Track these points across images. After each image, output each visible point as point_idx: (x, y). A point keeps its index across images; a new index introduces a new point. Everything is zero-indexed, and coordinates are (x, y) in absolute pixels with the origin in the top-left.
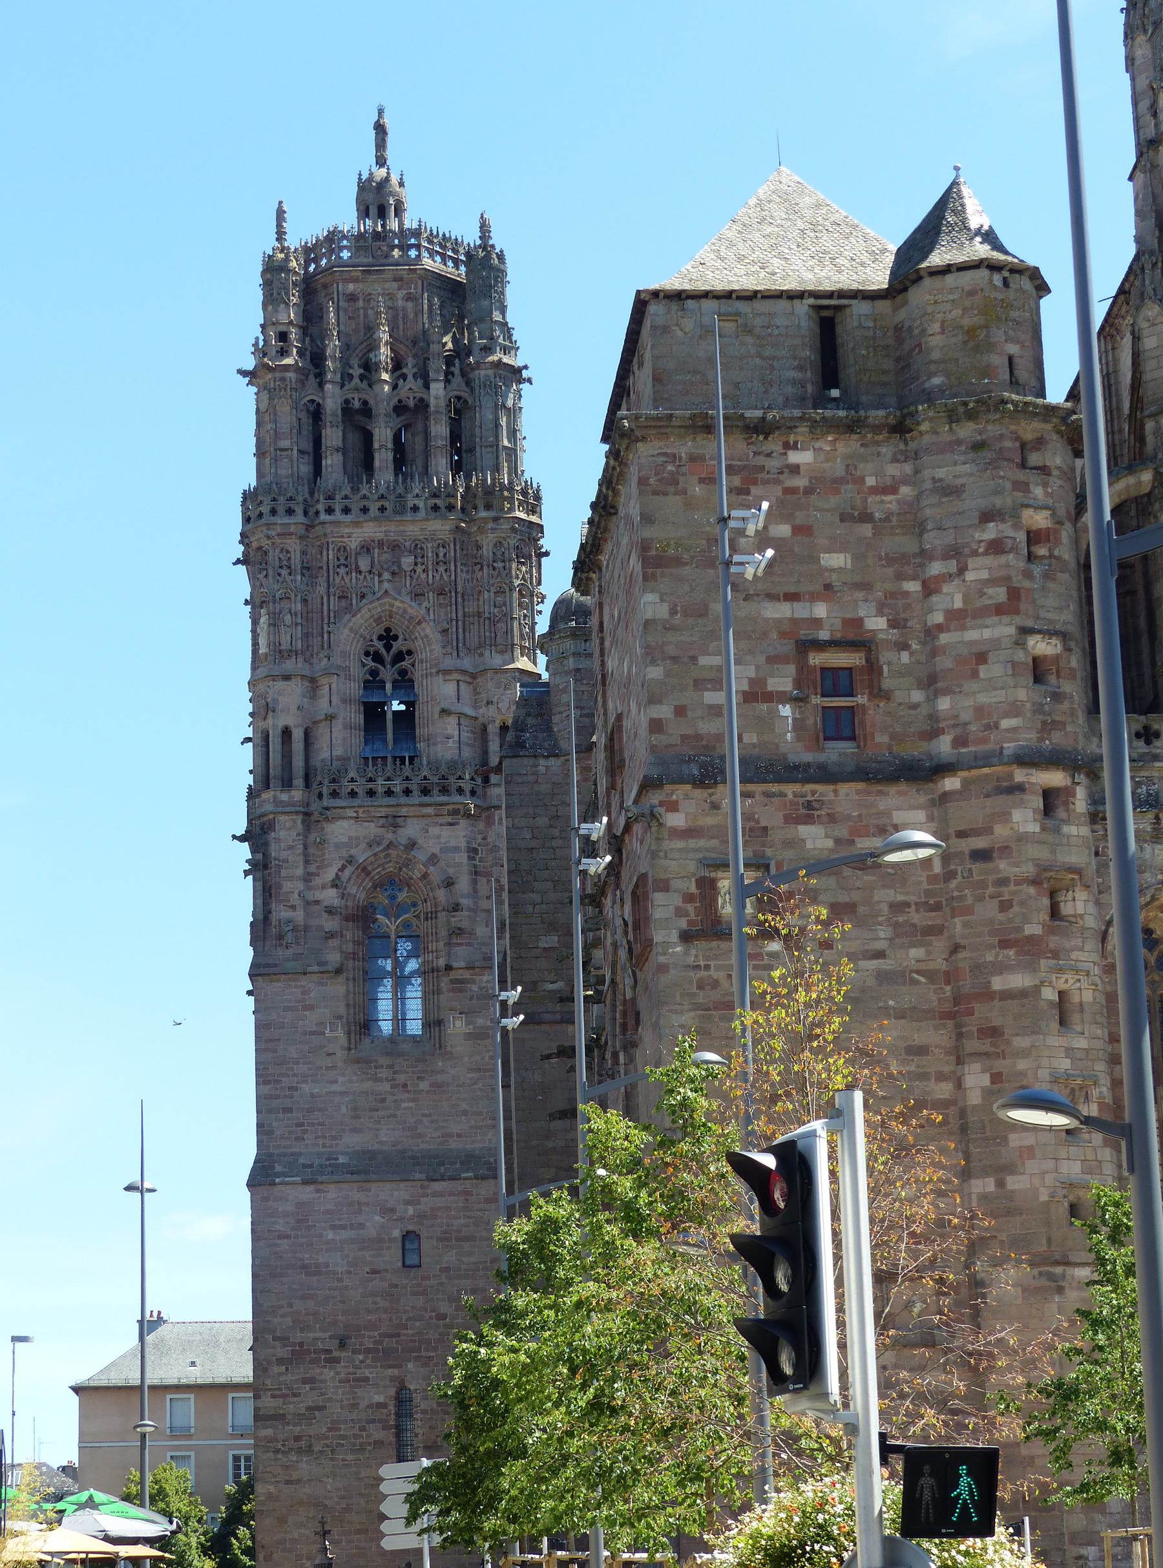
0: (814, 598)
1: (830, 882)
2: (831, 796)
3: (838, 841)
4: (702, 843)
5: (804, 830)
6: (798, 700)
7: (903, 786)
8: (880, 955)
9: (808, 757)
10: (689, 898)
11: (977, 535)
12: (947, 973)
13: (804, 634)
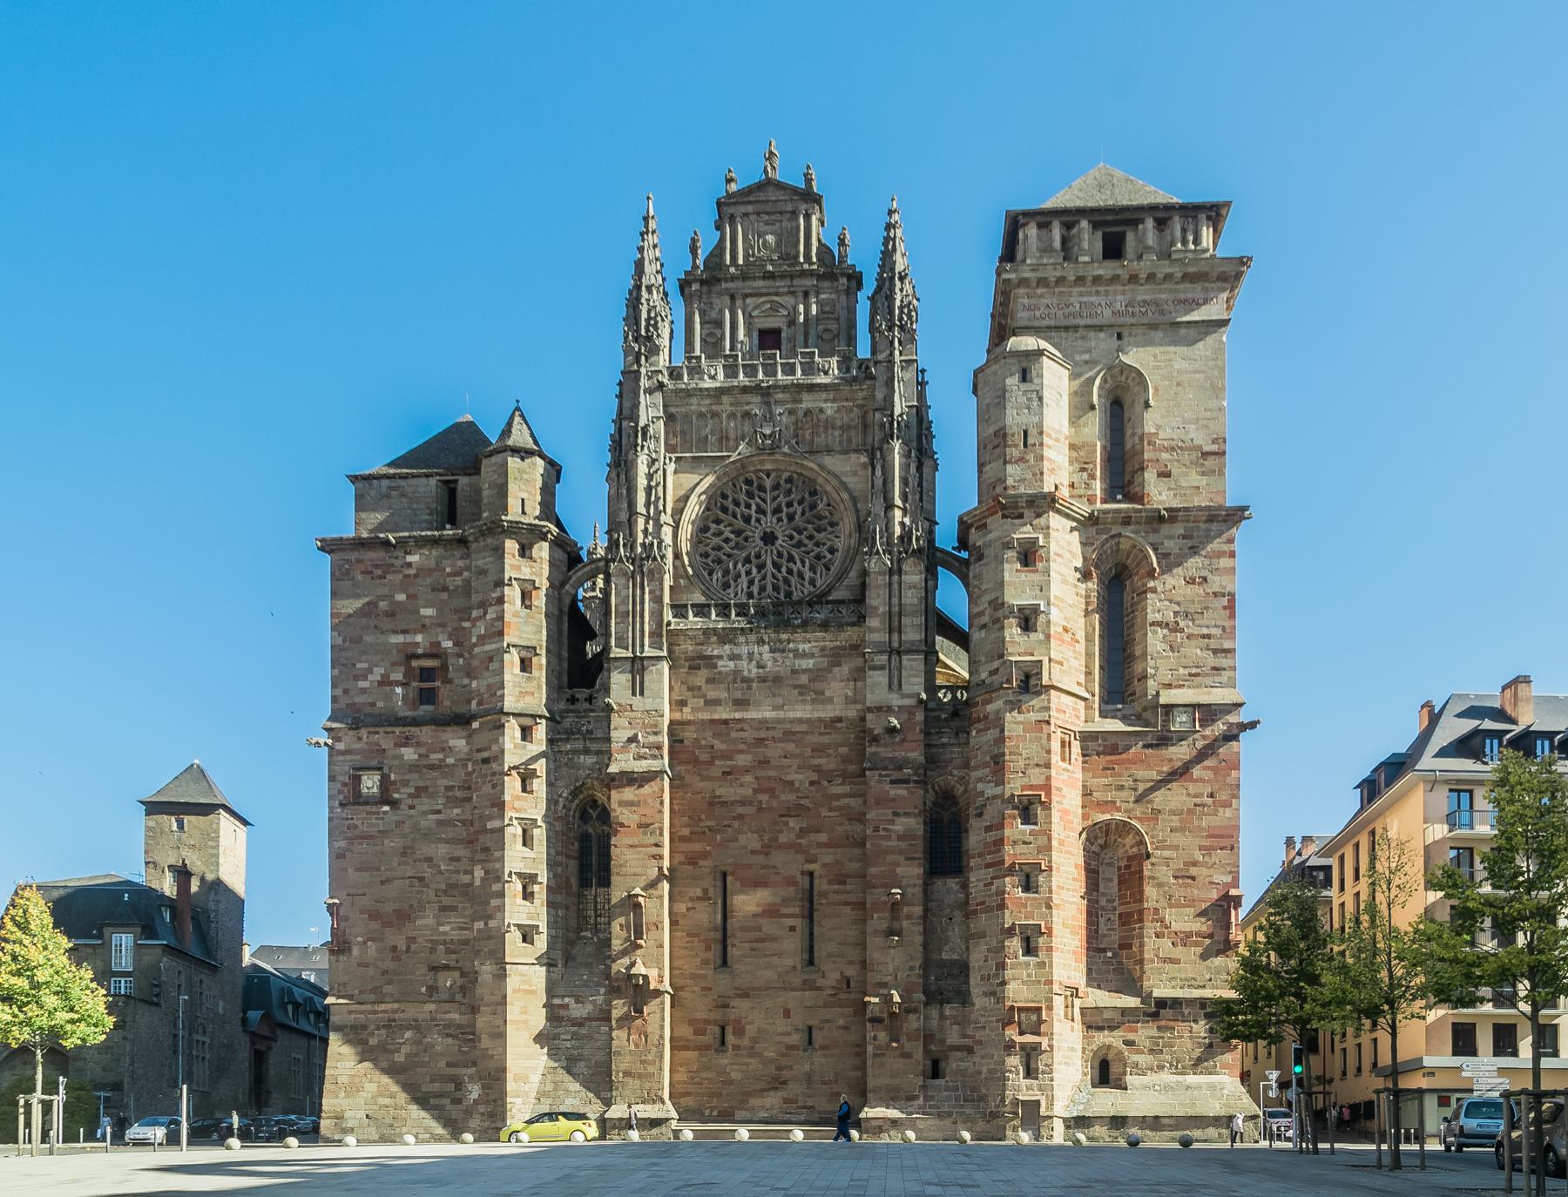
1: (416, 776)
3: (420, 755)
4: (352, 757)
5: (403, 750)
6: (403, 684)
7: (455, 728)
8: (439, 812)
9: (408, 714)
10: (345, 785)
13: (410, 650)
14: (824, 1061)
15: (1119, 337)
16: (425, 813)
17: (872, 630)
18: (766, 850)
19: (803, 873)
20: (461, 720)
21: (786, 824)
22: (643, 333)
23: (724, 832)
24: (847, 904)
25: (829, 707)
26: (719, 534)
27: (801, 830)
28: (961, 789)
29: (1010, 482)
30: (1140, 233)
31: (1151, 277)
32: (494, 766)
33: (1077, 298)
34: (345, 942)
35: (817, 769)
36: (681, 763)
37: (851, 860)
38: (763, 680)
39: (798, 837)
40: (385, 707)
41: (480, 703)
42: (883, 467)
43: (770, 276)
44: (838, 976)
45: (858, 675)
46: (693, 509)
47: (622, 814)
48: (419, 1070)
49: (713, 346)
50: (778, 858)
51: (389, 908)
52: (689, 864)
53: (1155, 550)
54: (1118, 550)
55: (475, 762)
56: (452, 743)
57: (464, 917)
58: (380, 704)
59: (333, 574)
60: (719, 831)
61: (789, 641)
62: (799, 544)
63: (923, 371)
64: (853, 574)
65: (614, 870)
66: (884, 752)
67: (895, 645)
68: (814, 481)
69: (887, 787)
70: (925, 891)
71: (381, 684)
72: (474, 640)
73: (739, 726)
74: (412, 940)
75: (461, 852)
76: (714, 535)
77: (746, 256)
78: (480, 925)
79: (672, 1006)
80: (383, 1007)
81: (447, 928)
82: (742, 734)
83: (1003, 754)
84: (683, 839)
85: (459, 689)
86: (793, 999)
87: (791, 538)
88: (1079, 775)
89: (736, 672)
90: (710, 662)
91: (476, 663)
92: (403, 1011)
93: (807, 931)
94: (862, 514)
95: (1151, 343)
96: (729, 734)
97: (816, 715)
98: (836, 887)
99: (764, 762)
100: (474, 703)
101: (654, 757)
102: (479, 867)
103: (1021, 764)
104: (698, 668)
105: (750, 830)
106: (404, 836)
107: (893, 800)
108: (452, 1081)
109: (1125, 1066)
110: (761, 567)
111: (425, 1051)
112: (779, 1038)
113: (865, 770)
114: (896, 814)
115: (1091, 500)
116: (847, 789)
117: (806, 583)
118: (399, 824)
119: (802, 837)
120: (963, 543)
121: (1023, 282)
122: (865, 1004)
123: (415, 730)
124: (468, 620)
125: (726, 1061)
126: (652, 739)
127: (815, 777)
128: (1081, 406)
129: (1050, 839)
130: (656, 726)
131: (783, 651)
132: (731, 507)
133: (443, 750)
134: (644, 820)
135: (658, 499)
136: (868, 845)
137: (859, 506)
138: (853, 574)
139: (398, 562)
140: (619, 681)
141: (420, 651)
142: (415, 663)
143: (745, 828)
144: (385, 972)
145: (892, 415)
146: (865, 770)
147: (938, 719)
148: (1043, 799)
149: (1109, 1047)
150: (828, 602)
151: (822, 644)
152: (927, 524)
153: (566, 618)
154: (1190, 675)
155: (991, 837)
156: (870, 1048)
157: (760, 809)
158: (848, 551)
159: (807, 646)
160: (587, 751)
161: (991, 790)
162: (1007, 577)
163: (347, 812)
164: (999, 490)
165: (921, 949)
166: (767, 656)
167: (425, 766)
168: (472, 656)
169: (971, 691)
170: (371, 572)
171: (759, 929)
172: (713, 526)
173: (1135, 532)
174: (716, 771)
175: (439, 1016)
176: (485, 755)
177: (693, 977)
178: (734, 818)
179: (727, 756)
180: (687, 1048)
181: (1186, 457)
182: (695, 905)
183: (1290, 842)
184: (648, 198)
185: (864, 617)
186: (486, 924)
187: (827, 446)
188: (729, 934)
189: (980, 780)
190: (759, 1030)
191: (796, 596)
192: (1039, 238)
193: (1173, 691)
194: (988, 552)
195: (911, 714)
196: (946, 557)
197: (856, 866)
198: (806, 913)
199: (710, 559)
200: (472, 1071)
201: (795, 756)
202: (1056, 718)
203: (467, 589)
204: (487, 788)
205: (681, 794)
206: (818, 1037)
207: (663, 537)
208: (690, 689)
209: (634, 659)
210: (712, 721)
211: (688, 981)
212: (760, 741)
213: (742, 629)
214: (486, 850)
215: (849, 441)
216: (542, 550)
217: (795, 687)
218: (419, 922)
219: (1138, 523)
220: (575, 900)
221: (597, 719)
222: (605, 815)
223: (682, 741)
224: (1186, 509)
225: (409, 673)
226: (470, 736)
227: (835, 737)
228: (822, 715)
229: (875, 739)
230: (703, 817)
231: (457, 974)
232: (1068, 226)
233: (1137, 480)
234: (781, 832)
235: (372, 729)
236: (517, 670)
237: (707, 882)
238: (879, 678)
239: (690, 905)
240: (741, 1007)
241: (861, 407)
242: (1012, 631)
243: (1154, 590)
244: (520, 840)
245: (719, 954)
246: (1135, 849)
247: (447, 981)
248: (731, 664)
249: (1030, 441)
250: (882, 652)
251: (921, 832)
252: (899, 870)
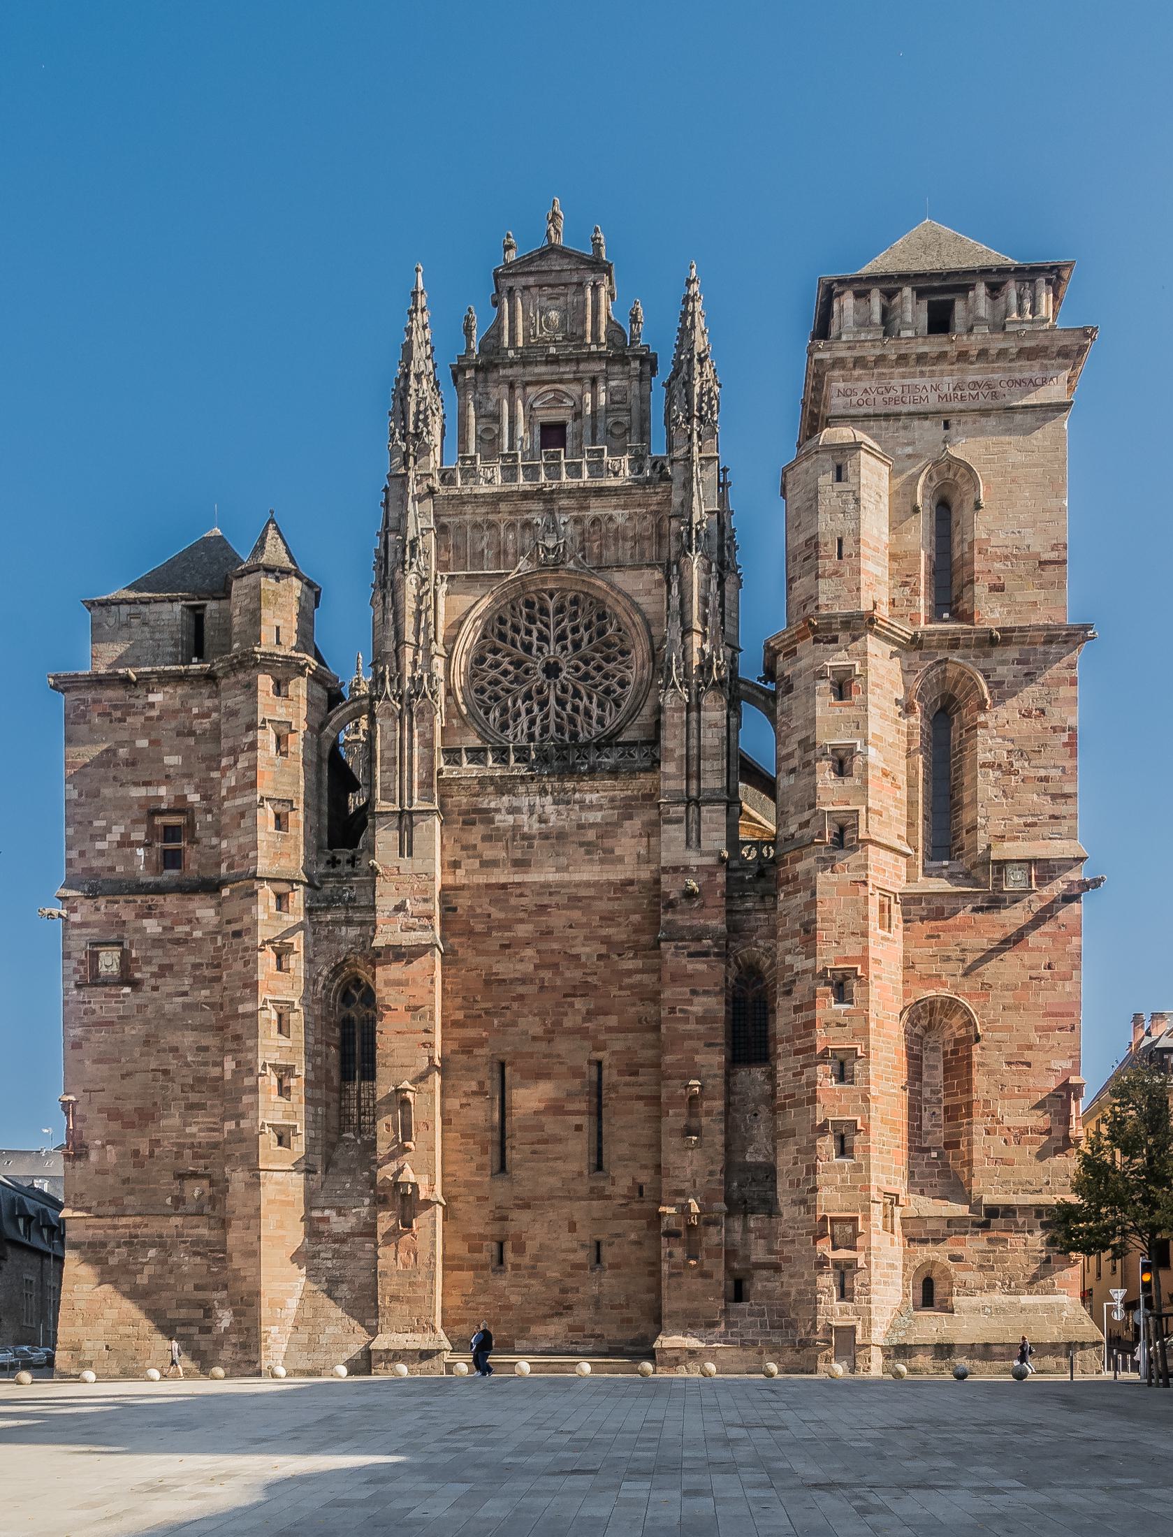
0: (159, 784)
2: (162, 902)
3: (164, 928)
4: (89, 931)
5: (146, 922)
6: (147, 846)
8: (185, 994)
9: (151, 879)
10: (81, 963)
11: (245, 740)
12: (221, 1004)
14: (613, 1281)
15: (947, 425)
16: (169, 995)
17: (668, 777)
18: (550, 1035)
19: (590, 1062)
20: (210, 887)
21: (572, 1005)
22: (411, 429)
23: (502, 1015)
24: (639, 1098)
25: (619, 867)
26: (496, 665)
27: (588, 1012)
28: (768, 962)
29: (822, 600)
30: (970, 302)
31: (983, 353)
32: (246, 939)
33: (898, 381)
34: (82, 1146)
35: (606, 941)
36: (454, 935)
37: (644, 1047)
38: (545, 836)
39: (585, 1020)
40: (126, 872)
41: (230, 867)
42: (680, 584)
43: (554, 360)
44: (629, 1183)
45: (652, 830)
46: (468, 638)
47: (384, 993)
48: (164, 1294)
49: (489, 443)
50: (562, 1046)
51: (129, 1106)
52: (463, 1052)
53: (987, 677)
54: (944, 678)
55: (225, 936)
56: (199, 913)
57: (214, 1116)
58: (119, 869)
59: (67, 717)
60: (496, 1014)
61: (574, 791)
62: (586, 677)
63: (725, 470)
64: (646, 711)
65: (378, 1060)
66: (682, 920)
67: (694, 793)
68: (603, 602)
69: (684, 961)
70: (727, 1083)
71: (121, 844)
72: (224, 793)
73: (518, 891)
74: (156, 1143)
75: (210, 1040)
76: (491, 666)
77: (527, 337)
78: (230, 1125)
79: (445, 1219)
80: (124, 1221)
81: (193, 1129)
82: (523, 901)
83: (815, 921)
84: (456, 1024)
85: (207, 850)
86: (578, 1210)
87: (577, 669)
88: (900, 946)
89: (516, 828)
90: (486, 815)
91: (225, 820)
92: (146, 1226)
93: (595, 1129)
94: (657, 640)
95: (982, 432)
96: (507, 901)
97: (605, 877)
98: (628, 1078)
99: (547, 933)
100: (224, 866)
101: (424, 928)
102: (230, 1057)
103: (835, 932)
104: (474, 824)
105: (530, 1012)
106: (147, 1022)
107: (691, 976)
108: (200, 1306)
109: (951, 1285)
110: (543, 704)
111: (171, 1272)
112: (563, 1256)
113: (659, 941)
114: (694, 992)
115: (914, 621)
116: (639, 963)
117: (594, 722)
118: (141, 1008)
119: (590, 1021)
120: (770, 674)
121: (838, 363)
122: (660, 1216)
123: (159, 899)
124: (218, 769)
125: (504, 1283)
126: (422, 907)
127: (603, 950)
128: (903, 510)
129: (867, 1020)
130: (426, 891)
131: (568, 803)
132: (510, 634)
133: (190, 921)
134: (413, 1002)
135: (428, 625)
136: (663, 1030)
137: (654, 630)
138: (646, 711)
139: (140, 702)
140: (385, 837)
141: (164, 806)
142: (159, 821)
143: (525, 1011)
144: (126, 1181)
145: (690, 523)
146: (659, 941)
147: (742, 879)
148: (859, 973)
149: (934, 1263)
150: (618, 744)
151: (611, 793)
152: (729, 651)
153: (325, 767)
154: (1026, 825)
155: (801, 1017)
156: (665, 1267)
157: (542, 988)
158: (641, 684)
159: (595, 796)
160: (349, 922)
161: (800, 963)
162: (819, 712)
163: (83, 995)
164: (810, 609)
165: (722, 1150)
166: (550, 809)
167: (169, 941)
168: (222, 812)
169: (779, 847)
170: (109, 714)
171: (541, 1128)
172: (490, 656)
173: (964, 657)
174: (493, 944)
175: (186, 1232)
176: (236, 927)
177: (468, 1184)
178: (514, 999)
179: (505, 926)
180: (460, 1268)
181: (1022, 568)
182: (470, 1101)
183: (1137, 1019)
184: (417, 270)
185: (658, 762)
186: (238, 1124)
187: (617, 560)
188: (508, 1134)
189: (788, 952)
190: (542, 1247)
191: (582, 737)
192: (856, 310)
193: (1006, 845)
194: (799, 684)
195: (712, 874)
196: (750, 690)
197: (649, 1054)
198: (594, 1109)
199: (487, 694)
200: (222, 1294)
201: (581, 926)
202: (874, 878)
203: (215, 734)
204: (238, 966)
205: (453, 971)
206: (607, 1253)
207: (434, 670)
208: (464, 848)
209: (401, 814)
210: (488, 886)
211: (462, 1189)
212: (542, 909)
213: (522, 777)
214: (237, 1038)
215: (642, 554)
216: (299, 688)
217: (582, 844)
218: (163, 1123)
219: (967, 646)
220: (336, 1095)
221: (361, 884)
222: (369, 996)
223: (455, 909)
224: (1021, 629)
225: (152, 832)
226: (220, 905)
227: (628, 903)
228: (612, 877)
229: (671, 905)
230: (479, 998)
231: (205, 1182)
232: (889, 295)
233: (966, 596)
234: (566, 1014)
235: (110, 898)
236: (271, 827)
237: (483, 1074)
238: (674, 833)
239: (464, 1101)
240: (521, 1219)
241: (655, 513)
242: (825, 775)
243: (985, 726)
244: (275, 1026)
245: (497, 1158)
246: (963, 1031)
247: (195, 1190)
248: (510, 818)
249: (845, 551)
250: (678, 803)
251: (723, 1014)
252: (698, 1058)
